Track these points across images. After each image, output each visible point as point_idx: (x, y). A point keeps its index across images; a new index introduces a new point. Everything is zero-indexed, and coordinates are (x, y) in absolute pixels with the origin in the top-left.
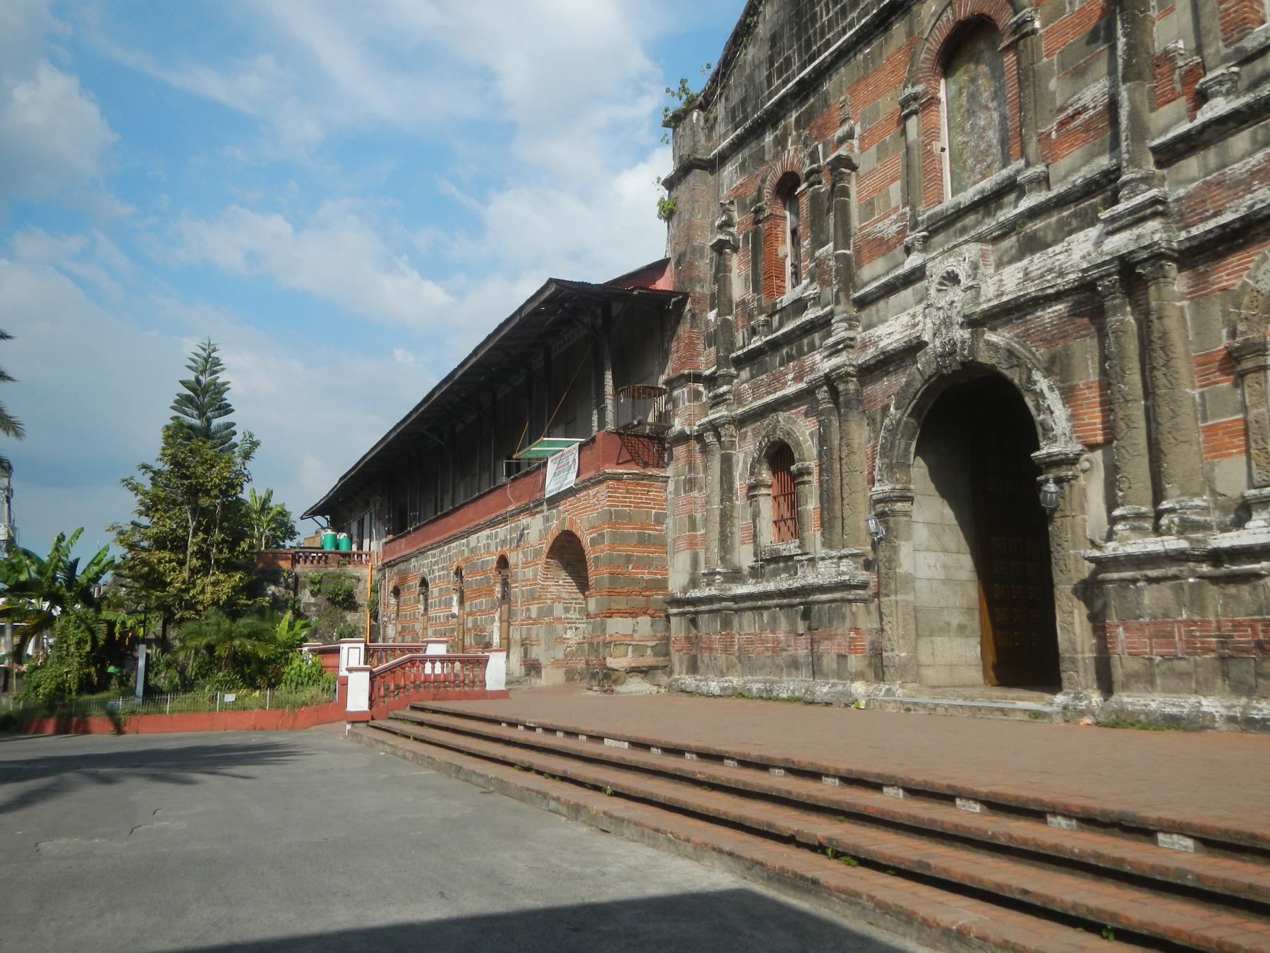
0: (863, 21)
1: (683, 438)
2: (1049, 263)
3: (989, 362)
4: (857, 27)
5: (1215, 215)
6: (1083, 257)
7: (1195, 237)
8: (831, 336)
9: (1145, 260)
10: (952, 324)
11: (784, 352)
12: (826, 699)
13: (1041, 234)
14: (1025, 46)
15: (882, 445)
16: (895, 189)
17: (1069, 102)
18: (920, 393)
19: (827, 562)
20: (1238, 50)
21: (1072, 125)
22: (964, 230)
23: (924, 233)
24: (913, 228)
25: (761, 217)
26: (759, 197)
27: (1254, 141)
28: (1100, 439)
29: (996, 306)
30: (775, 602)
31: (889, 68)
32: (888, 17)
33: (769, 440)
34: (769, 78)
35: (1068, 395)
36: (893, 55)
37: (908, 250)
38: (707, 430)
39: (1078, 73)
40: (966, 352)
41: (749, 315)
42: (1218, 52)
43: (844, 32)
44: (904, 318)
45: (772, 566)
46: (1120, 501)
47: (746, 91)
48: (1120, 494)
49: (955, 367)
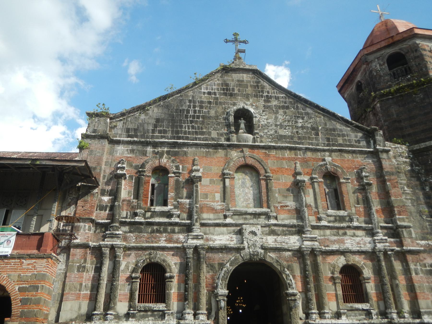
0: (210, 142)
1: (85, 246)
2: (283, 240)
3: (270, 262)
4: (207, 142)
5: (328, 246)
6: (294, 243)
7: (326, 250)
8: (191, 232)
9: (318, 251)
10: (256, 247)
11: (155, 228)
13: (277, 231)
14: (270, 182)
15: (223, 277)
16: (218, 196)
17: (283, 202)
18: (240, 263)
19: (191, 315)
20: (326, 214)
21: (285, 208)
22: (246, 219)
23: (232, 214)
24: (229, 210)
25: (145, 174)
26: (143, 166)
27: (331, 233)
28: (301, 290)
29: (274, 247)
31: (216, 160)
32: (218, 146)
33: (150, 261)
34: (153, 131)
35: (294, 277)
36: (219, 158)
37: (225, 217)
38: (107, 247)
39: (285, 197)
40: (262, 256)
41: (132, 207)
42: (322, 211)
43: (196, 139)
44: (227, 237)
45: (142, 313)
46: (312, 308)
47: (138, 127)
48: (313, 307)
49: (258, 259)
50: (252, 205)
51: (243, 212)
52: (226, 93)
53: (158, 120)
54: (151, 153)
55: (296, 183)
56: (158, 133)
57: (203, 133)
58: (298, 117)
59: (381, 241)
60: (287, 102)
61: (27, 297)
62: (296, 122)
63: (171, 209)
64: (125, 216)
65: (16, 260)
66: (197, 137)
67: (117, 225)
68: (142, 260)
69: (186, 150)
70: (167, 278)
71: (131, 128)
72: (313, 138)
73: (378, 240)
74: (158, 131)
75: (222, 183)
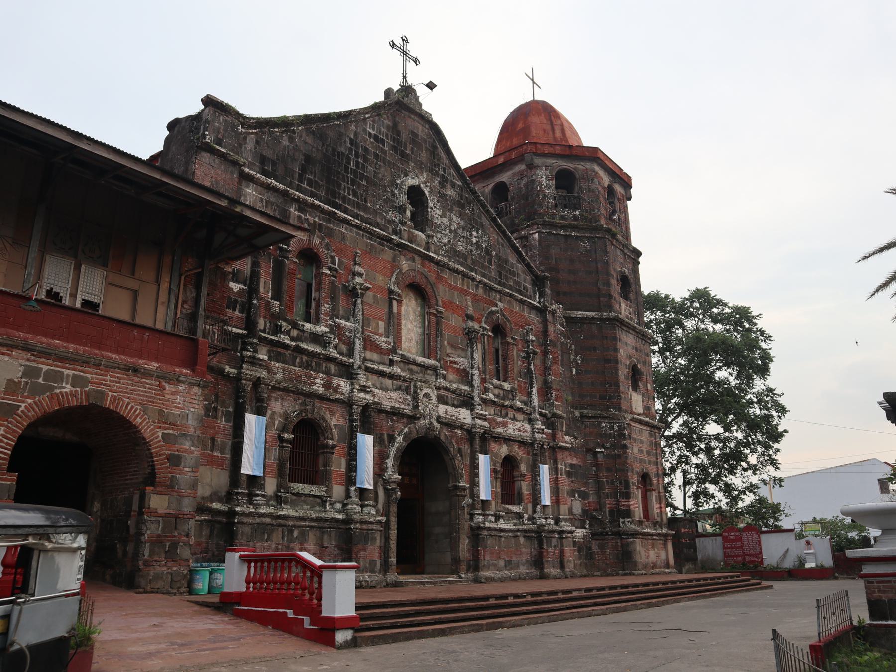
12: (373, 584)
17: (452, 355)
20: (492, 384)
24: (396, 353)
30: (307, 523)
37: (392, 363)
38: (250, 380)
50: (414, 350)
51: (411, 360)
52: (396, 147)
53: (308, 159)
54: (296, 219)
55: (467, 331)
56: (307, 185)
57: (366, 209)
58: (473, 227)
59: (541, 431)
60: (464, 197)
61: (177, 453)
62: (471, 235)
63: (325, 332)
64: (262, 327)
65: (153, 382)
66: (359, 212)
67: (256, 341)
68: (296, 413)
69: (343, 231)
70: (326, 446)
71: (268, 158)
72: (486, 266)
73: (537, 429)
74: (307, 180)
75: (387, 305)
